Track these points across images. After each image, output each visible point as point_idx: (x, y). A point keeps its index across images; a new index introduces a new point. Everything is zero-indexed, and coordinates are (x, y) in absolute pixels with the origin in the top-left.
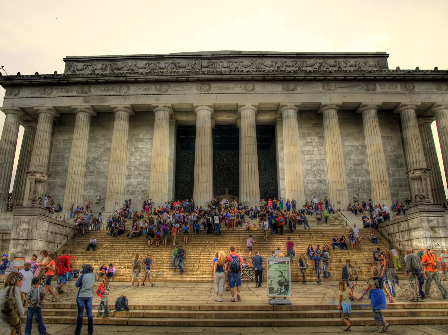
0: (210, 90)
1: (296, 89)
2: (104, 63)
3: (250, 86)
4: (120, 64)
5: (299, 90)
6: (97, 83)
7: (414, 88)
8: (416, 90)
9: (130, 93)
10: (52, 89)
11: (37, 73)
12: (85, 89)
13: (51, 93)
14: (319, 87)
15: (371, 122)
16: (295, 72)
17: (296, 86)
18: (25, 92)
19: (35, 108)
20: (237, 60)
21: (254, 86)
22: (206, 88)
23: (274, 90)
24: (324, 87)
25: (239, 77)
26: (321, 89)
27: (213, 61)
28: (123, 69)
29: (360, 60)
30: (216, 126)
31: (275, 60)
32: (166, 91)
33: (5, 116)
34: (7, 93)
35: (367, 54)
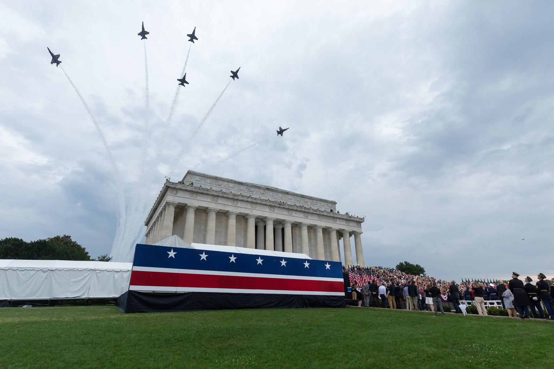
1: (307, 217)
3: (290, 212)
4: (220, 183)
5: (309, 217)
12: (216, 198)
25: (287, 207)
26: (317, 218)
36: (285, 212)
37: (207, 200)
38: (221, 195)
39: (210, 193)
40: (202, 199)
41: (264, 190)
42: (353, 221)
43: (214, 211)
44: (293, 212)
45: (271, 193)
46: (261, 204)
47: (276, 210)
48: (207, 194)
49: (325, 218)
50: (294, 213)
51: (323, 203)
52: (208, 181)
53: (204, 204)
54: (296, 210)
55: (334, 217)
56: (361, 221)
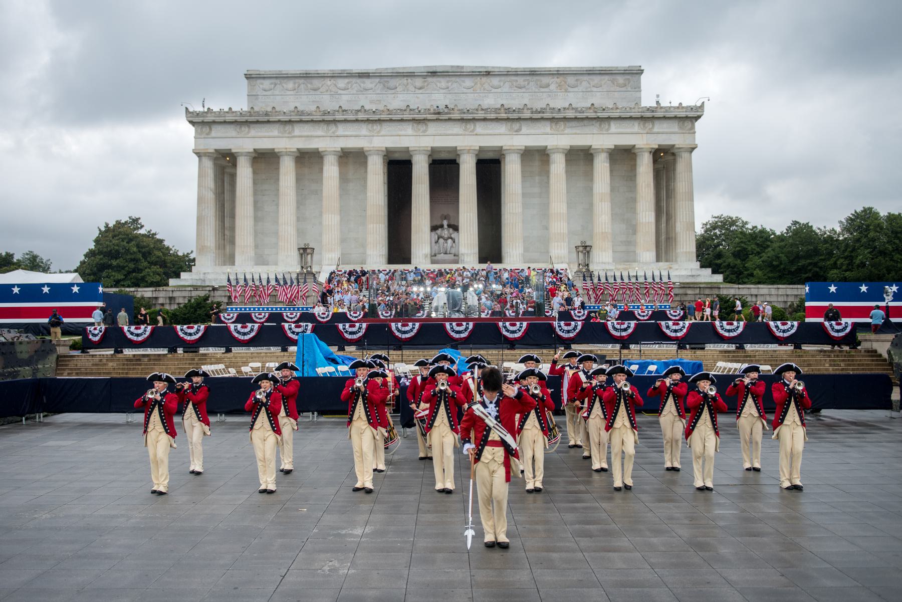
0: (425, 131)
1: (520, 130)
2: (297, 80)
3: (470, 126)
4: (316, 83)
6: (301, 121)
7: (653, 127)
8: (656, 130)
9: (337, 134)
10: (249, 127)
11: (230, 109)
12: (288, 127)
13: (248, 132)
14: (546, 127)
15: (602, 166)
16: (520, 111)
17: (521, 127)
18: (217, 131)
19: (233, 151)
20: (457, 79)
21: (475, 126)
22: (422, 129)
23: (497, 132)
24: (551, 127)
25: (456, 116)
27: (430, 79)
28: (321, 90)
29: (606, 77)
30: (433, 161)
31: (503, 78)
32: (379, 132)
33: (197, 159)
34: (196, 131)
35: (617, 69)
36: (457, 128)
37: (271, 134)
38: (297, 118)
39: (272, 119)
40: (260, 134)
41: (424, 77)
42: (665, 118)
43: (288, 154)
44: (478, 124)
45: (443, 82)
46: (391, 120)
47: (433, 128)
48: (268, 122)
49: (573, 124)
50: (480, 128)
51: (596, 79)
52: (290, 85)
53: (265, 144)
54: (485, 120)
55: (598, 119)
56: (691, 114)
